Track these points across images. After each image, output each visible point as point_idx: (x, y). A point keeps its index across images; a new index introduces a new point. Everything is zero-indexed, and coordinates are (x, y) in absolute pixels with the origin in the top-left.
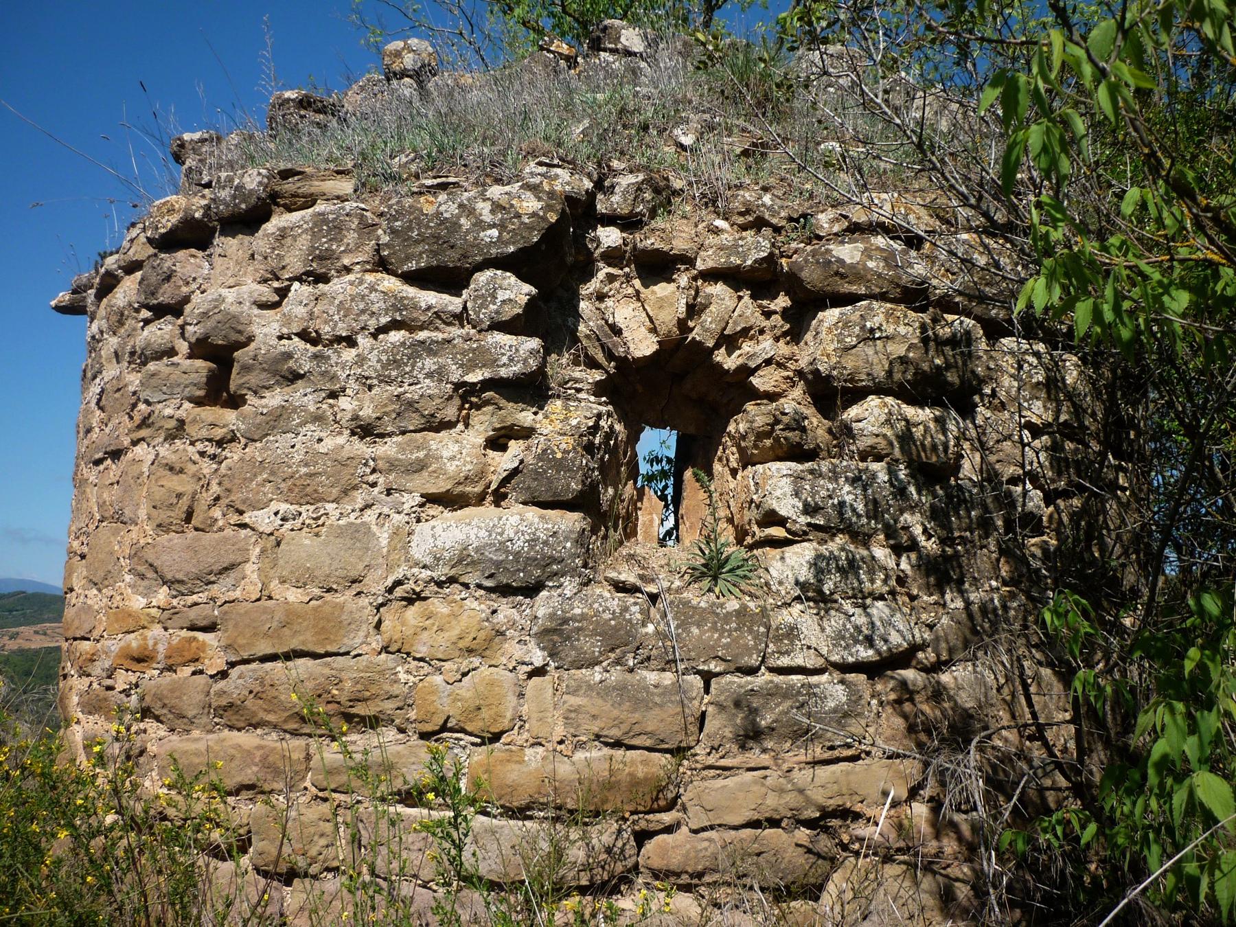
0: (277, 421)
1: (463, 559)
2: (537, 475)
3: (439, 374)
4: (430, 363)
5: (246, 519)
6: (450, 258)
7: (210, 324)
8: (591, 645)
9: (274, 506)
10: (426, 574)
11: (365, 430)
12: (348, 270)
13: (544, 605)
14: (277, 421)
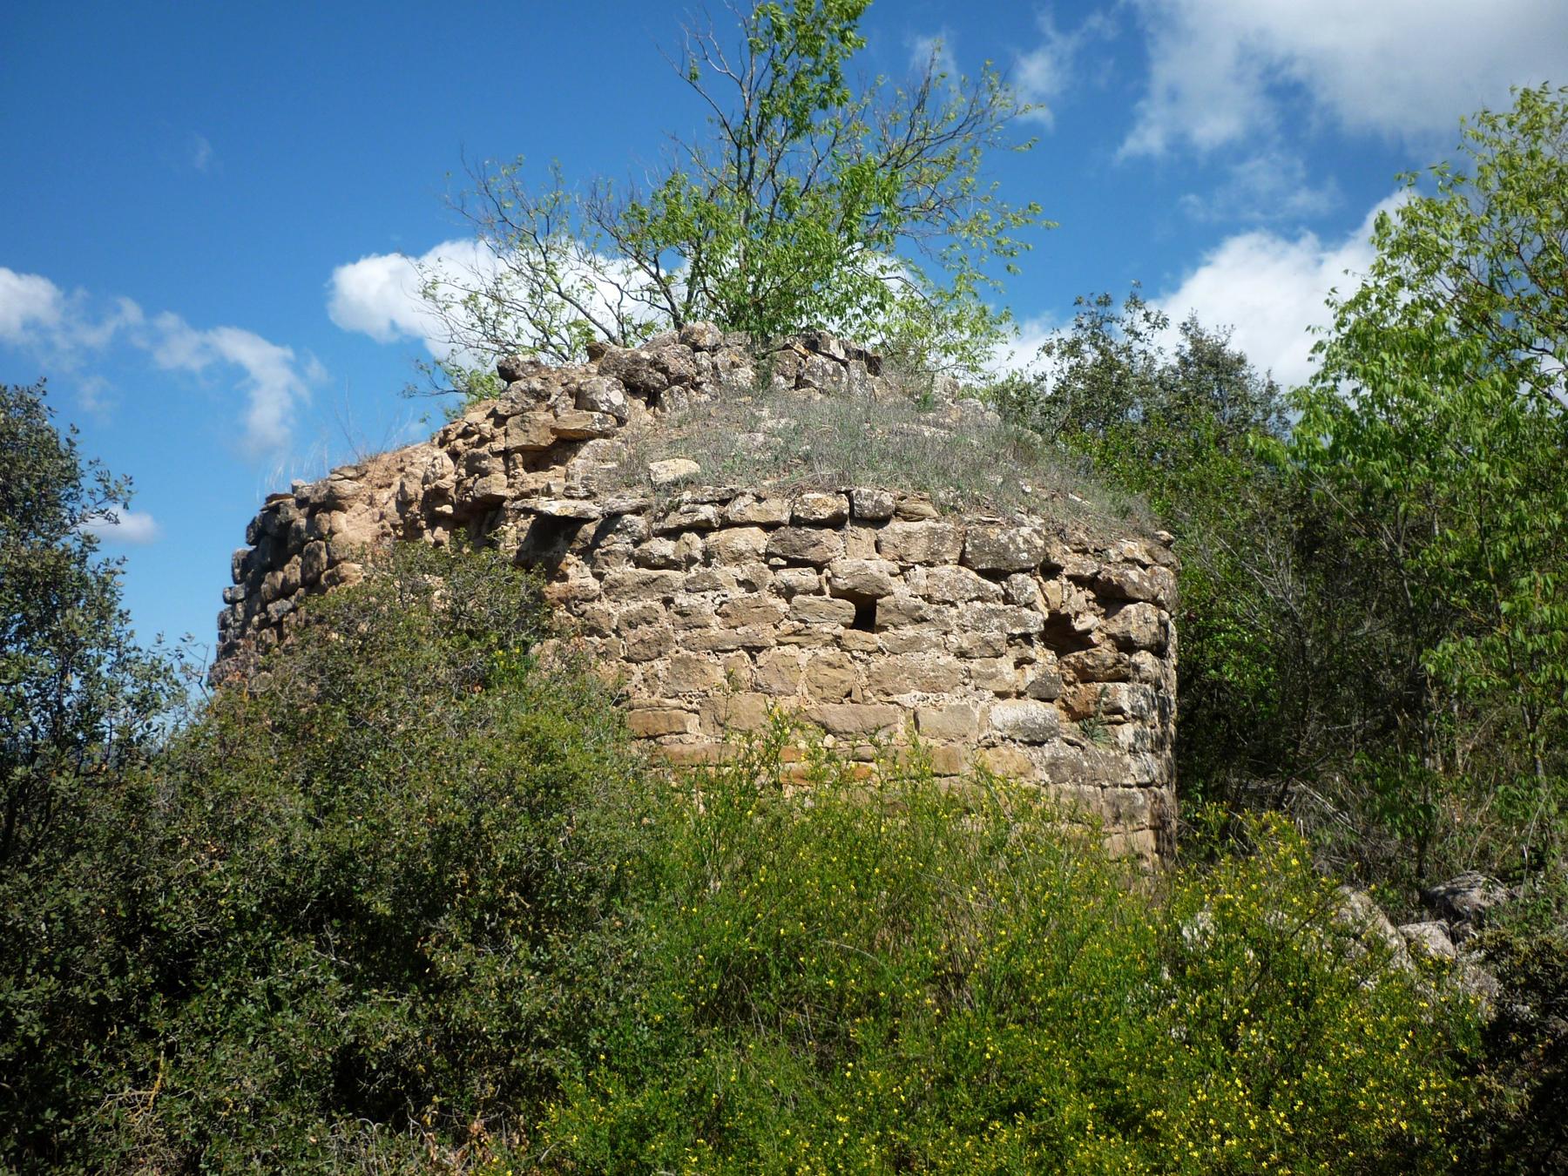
0: (913, 644)
1: (1017, 727)
2: (1042, 685)
3: (1001, 628)
4: (996, 621)
5: (895, 698)
6: (1003, 565)
7: (857, 580)
8: (1066, 771)
9: (914, 692)
10: (999, 734)
11: (962, 654)
12: (946, 562)
13: (1048, 751)
14: (913, 644)
